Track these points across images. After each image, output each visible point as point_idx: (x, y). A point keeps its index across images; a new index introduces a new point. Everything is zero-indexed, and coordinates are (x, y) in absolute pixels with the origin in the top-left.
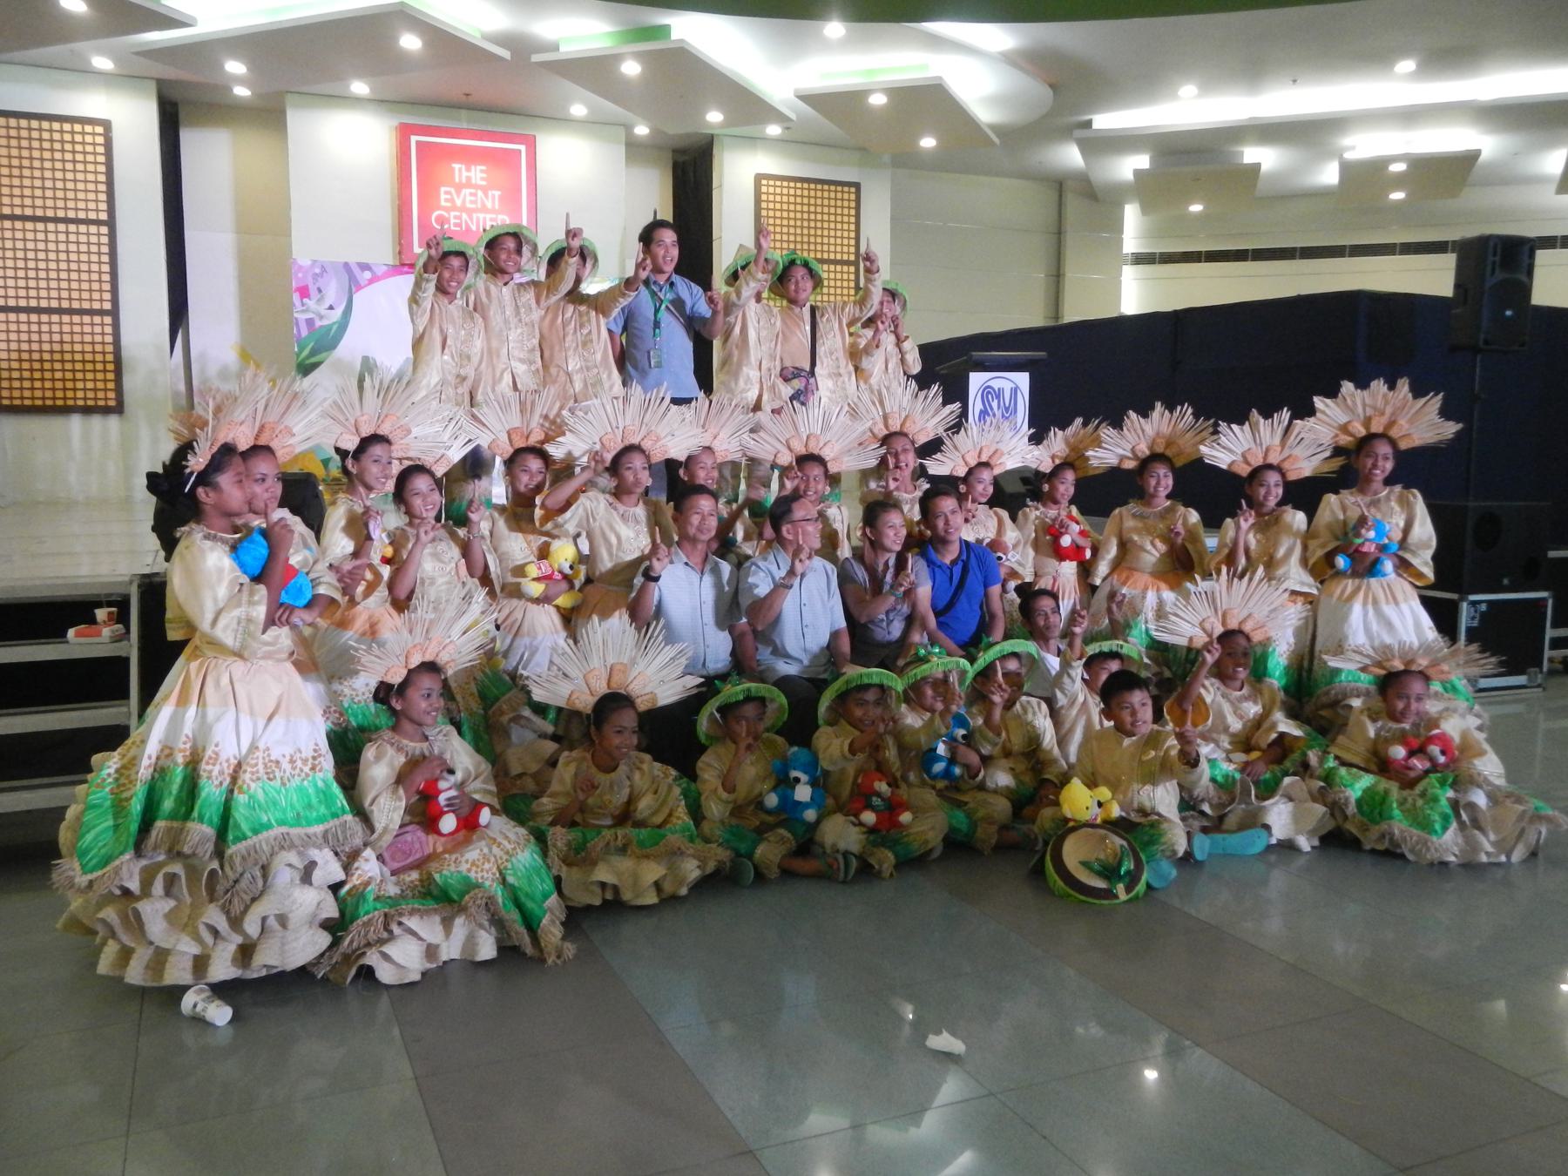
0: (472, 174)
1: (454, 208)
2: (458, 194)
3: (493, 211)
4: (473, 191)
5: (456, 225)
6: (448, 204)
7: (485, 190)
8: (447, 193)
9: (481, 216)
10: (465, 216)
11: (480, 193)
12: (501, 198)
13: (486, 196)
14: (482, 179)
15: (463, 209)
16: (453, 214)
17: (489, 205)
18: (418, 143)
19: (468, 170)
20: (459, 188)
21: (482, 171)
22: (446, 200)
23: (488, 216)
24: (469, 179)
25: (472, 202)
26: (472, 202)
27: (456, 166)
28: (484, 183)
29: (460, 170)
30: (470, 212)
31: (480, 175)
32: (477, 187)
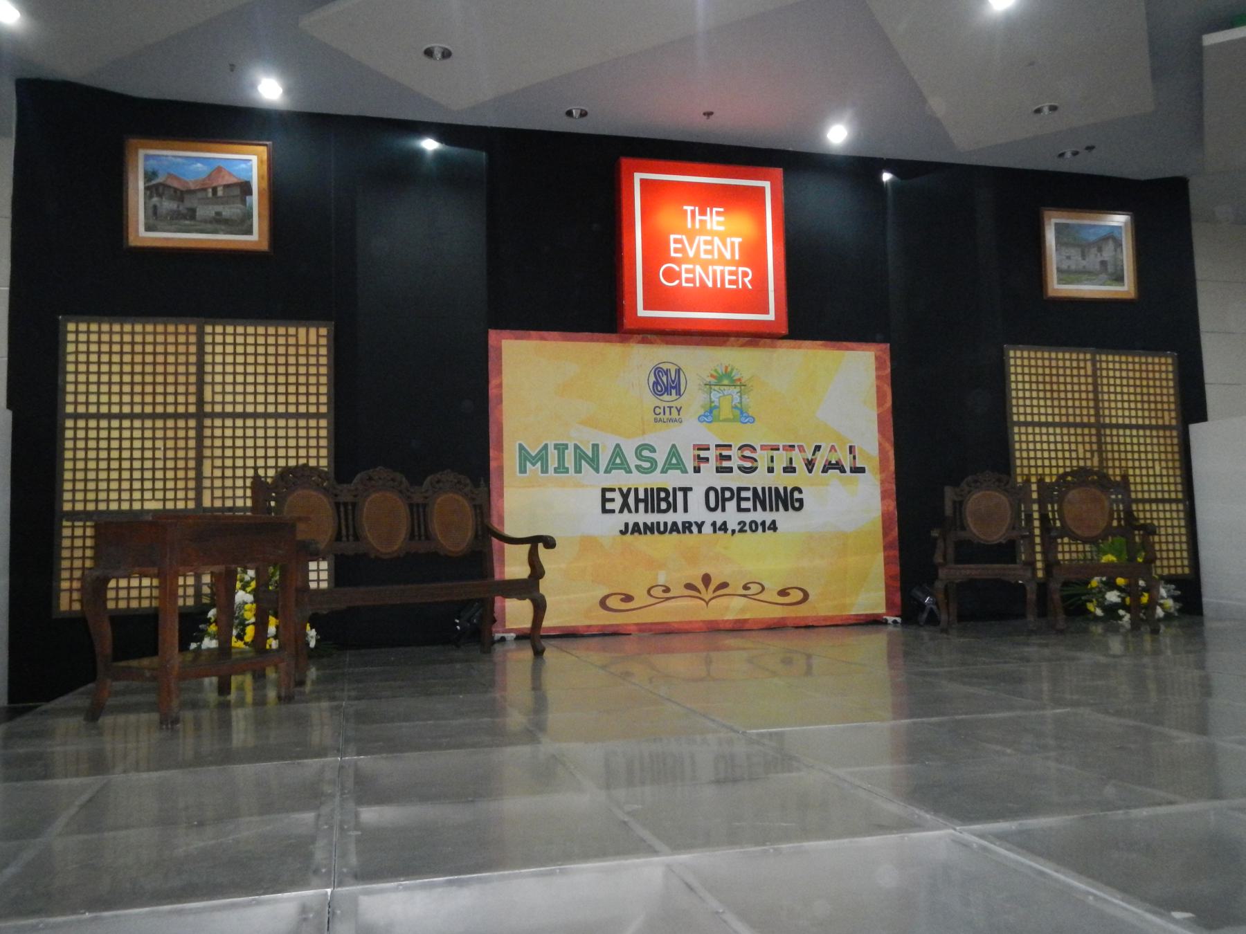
0: (707, 218)
1: (686, 260)
2: (691, 246)
4: (709, 238)
5: (687, 280)
6: (679, 255)
8: (676, 241)
9: (718, 268)
10: (698, 269)
11: (717, 241)
12: (741, 245)
13: (724, 244)
15: (696, 260)
17: (728, 256)
18: (643, 181)
19: (703, 213)
20: (691, 235)
21: (718, 213)
22: (676, 250)
23: (727, 269)
25: (706, 252)
26: (706, 252)
27: (689, 208)
28: (722, 228)
30: (705, 265)
32: (712, 233)
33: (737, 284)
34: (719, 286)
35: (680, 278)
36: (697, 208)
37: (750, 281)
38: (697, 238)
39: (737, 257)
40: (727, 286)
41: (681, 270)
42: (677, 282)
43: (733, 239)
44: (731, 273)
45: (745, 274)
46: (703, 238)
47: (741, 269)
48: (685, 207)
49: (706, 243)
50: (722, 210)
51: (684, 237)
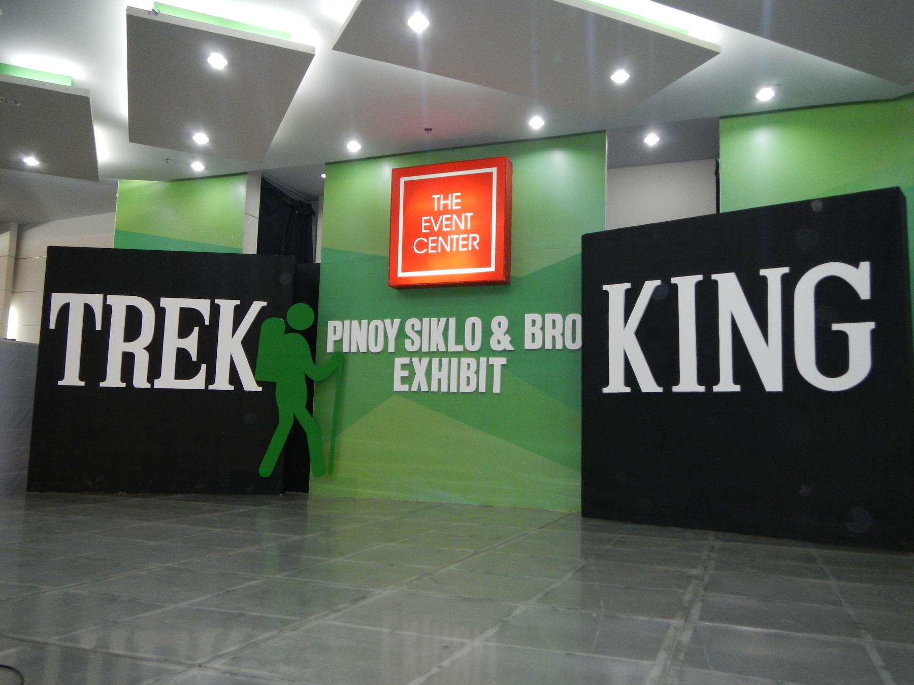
0: (449, 202)
3: (466, 231)
5: (433, 248)
7: (459, 213)
8: (426, 221)
9: (455, 237)
14: (457, 204)
15: (440, 233)
16: (430, 238)
17: (462, 227)
19: (446, 198)
20: (437, 215)
21: (457, 197)
22: (426, 228)
23: (461, 236)
24: (446, 206)
25: (447, 226)
27: (436, 197)
29: (439, 199)
31: (455, 201)
32: (452, 212)
33: (468, 247)
34: (454, 249)
35: (427, 247)
36: (442, 196)
37: (478, 244)
38: (441, 216)
39: (469, 227)
40: (461, 249)
41: (428, 240)
42: (425, 250)
43: (467, 214)
44: (464, 239)
45: (474, 239)
46: (445, 216)
47: (471, 235)
48: (433, 196)
49: (447, 219)
50: (459, 194)
51: (432, 218)
